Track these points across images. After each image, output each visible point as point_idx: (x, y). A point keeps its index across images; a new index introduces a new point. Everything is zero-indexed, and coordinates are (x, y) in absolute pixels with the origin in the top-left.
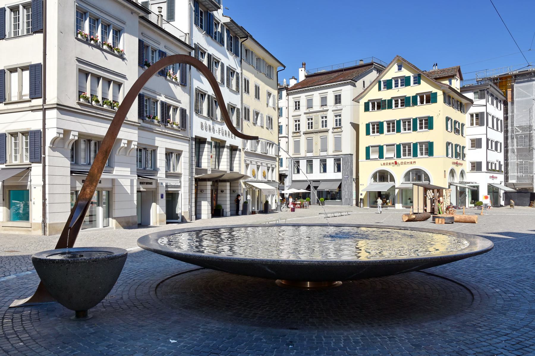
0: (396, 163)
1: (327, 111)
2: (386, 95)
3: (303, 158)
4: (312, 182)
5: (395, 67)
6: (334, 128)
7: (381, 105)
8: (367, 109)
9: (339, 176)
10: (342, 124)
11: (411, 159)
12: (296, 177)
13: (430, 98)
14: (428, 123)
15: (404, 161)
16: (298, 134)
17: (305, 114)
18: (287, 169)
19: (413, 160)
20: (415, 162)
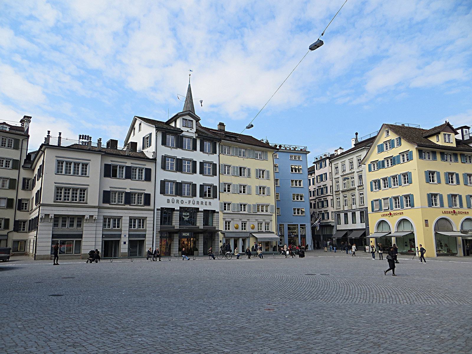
0: (390, 214)
1: (354, 172)
2: (381, 157)
3: (342, 212)
4: (348, 231)
5: (385, 134)
6: (358, 187)
7: (381, 165)
8: (370, 170)
9: (363, 226)
10: (363, 184)
11: (399, 210)
12: (339, 227)
13: (408, 156)
14: (407, 177)
15: (395, 212)
16: (339, 193)
17: (342, 176)
18: (333, 221)
19: (401, 212)
20: (402, 213)
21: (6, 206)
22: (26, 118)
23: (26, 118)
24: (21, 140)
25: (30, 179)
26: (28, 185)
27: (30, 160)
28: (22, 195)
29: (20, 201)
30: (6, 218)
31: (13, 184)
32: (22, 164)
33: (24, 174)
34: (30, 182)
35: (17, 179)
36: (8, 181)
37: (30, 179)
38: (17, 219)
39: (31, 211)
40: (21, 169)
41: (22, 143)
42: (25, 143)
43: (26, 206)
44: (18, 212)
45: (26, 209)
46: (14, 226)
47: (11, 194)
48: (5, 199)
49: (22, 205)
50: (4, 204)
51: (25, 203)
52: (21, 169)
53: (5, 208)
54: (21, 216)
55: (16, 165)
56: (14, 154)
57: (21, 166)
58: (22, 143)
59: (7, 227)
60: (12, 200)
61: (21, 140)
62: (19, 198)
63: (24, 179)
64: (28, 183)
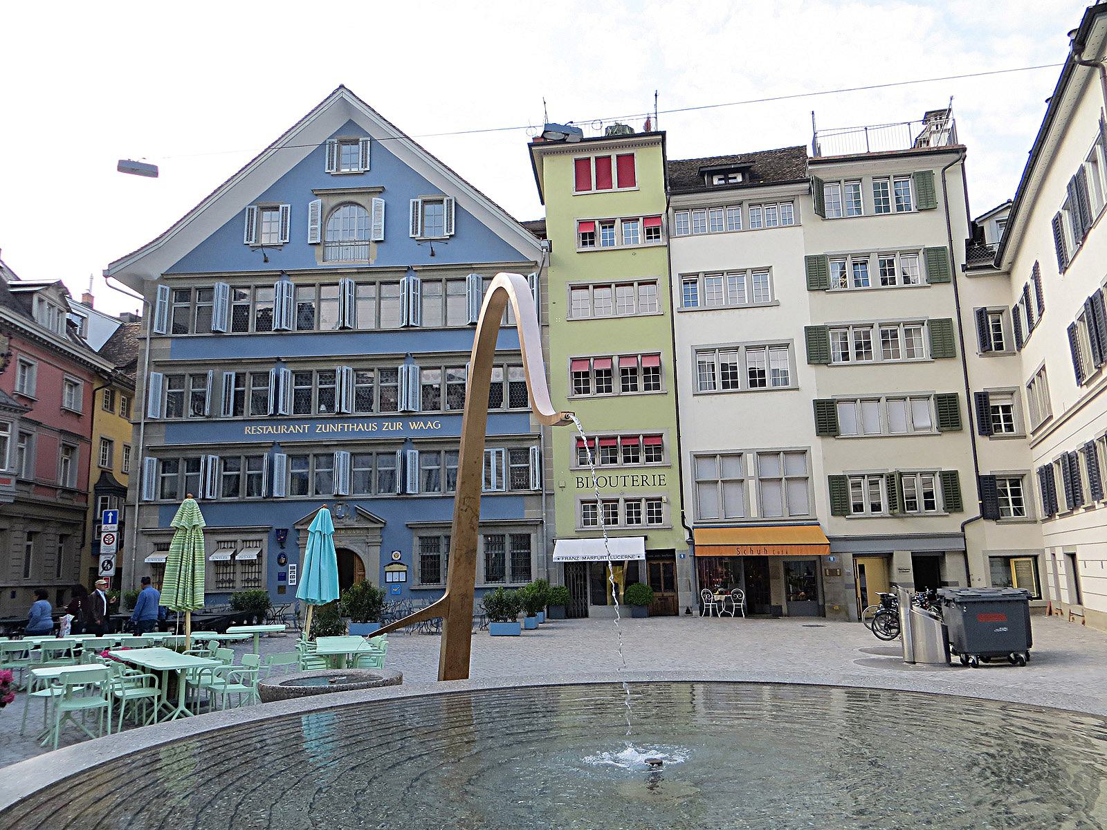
21: (935, 425)
22: (932, 120)
23: (932, 120)
24: (937, 173)
25: (1001, 312)
26: (998, 337)
27: (985, 250)
28: (987, 374)
29: (982, 398)
30: (947, 468)
31: (943, 341)
32: (961, 257)
33: (977, 292)
34: (1006, 323)
35: (955, 320)
36: (924, 330)
37: (1001, 312)
38: (984, 472)
39: (1033, 433)
40: (961, 277)
41: (944, 181)
42: (954, 180)
43: (1008, 419)
44: (982, 441)
45: (1010, 428)
46: (981, 497)
47: (944, 378)
48: (928, 398)
49: (992, 417)
50: (927, 416)
51: (1002, 406)
52: (961, 277)
53: (935, 431)
54: (998, 457)
55: (939, 267)
56: (924, 230)
57: (959, 269)
58: (944, 181)
59: (954, 503)
60: (953, 398)
61: (937, 173)
62: (977, 388)
63: (982, 314)
64: (998, 328)
